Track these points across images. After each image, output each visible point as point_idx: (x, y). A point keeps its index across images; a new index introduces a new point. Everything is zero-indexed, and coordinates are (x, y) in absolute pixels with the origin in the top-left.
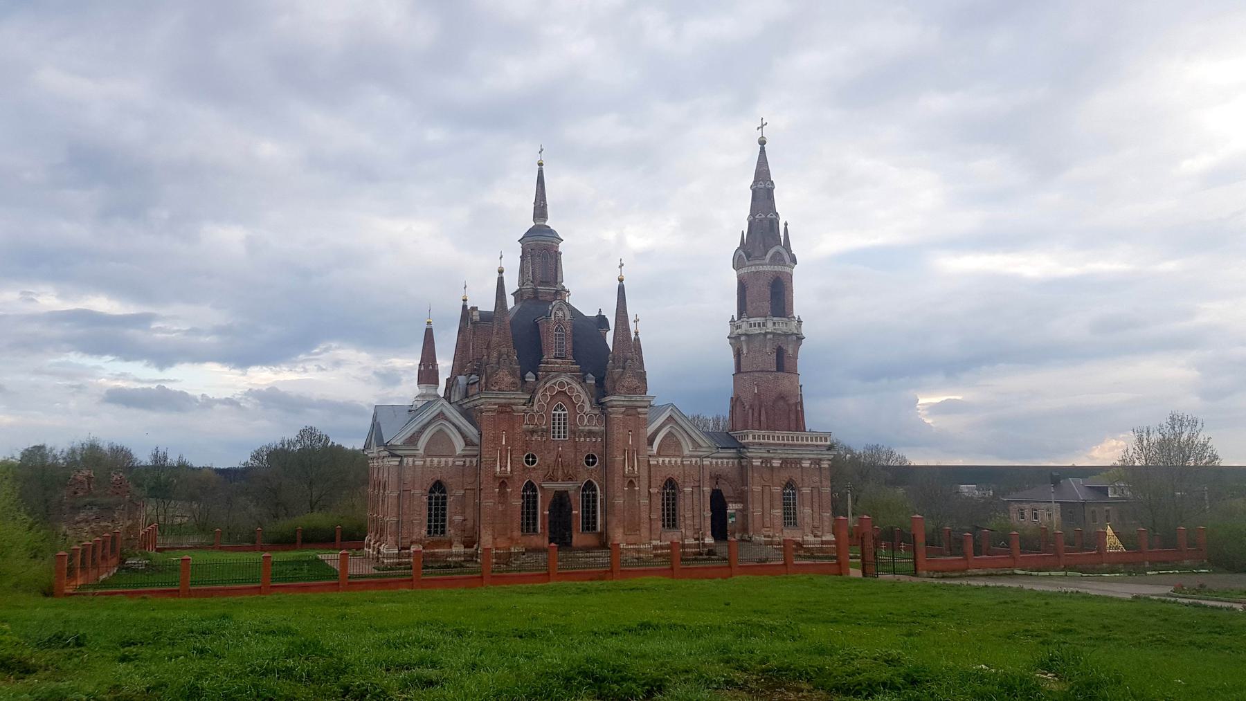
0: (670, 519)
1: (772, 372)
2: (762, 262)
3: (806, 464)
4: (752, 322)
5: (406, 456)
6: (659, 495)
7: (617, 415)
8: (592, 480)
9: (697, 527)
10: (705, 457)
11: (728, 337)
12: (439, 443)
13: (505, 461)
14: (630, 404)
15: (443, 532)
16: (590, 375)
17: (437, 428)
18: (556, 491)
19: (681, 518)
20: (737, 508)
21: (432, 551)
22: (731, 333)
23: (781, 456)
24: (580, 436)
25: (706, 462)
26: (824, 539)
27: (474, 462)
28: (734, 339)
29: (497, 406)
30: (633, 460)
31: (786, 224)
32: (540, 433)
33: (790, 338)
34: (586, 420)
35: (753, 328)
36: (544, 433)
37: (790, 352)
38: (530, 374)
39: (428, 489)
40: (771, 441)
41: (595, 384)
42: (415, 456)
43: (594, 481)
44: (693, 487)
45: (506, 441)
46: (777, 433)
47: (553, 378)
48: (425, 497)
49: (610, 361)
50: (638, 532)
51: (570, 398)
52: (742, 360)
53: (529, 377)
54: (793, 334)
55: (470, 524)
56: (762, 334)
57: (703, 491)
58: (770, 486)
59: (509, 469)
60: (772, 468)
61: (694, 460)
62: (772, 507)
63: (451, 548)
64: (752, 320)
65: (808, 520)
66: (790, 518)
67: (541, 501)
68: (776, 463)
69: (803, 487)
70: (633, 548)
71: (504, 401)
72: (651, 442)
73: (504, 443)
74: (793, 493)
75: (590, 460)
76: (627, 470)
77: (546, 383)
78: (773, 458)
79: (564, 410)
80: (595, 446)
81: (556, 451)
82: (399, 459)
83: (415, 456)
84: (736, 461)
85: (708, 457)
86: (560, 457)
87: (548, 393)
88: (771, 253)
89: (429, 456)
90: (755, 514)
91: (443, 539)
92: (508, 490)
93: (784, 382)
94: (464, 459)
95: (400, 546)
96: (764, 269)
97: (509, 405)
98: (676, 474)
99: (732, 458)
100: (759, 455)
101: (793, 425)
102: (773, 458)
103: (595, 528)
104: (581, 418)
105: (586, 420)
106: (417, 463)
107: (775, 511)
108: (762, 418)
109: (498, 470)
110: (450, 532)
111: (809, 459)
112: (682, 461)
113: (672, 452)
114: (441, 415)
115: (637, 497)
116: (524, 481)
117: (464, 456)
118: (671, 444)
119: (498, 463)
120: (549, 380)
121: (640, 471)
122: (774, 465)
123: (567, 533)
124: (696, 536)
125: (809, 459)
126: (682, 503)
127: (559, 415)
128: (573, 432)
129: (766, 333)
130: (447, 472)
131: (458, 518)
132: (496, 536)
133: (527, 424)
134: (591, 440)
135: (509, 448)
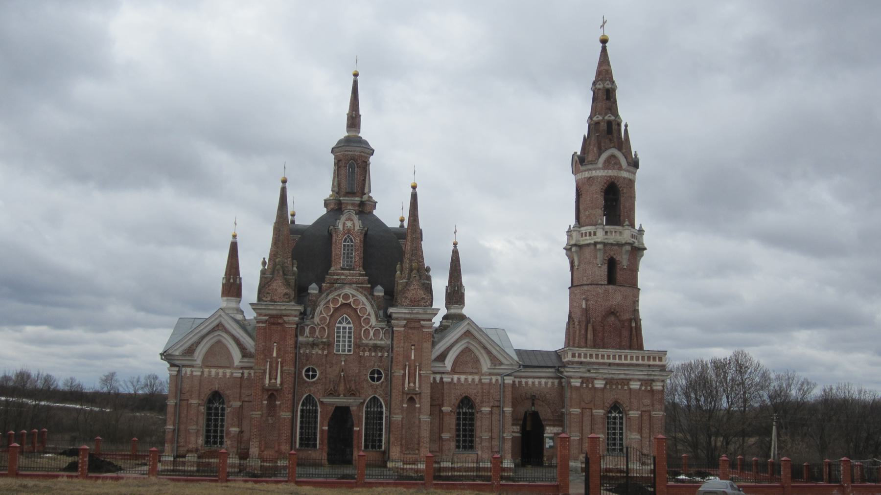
1: (602, 285)
3: (635, 385)
4: (584, 232)
5: (184, 366)
6: (452, 414)
8: (377, 396)
11: (564, 249)
12: (217, 353)
13: (275, 374)
14: (412, 316)
15: (221, 443)
16: (379, 287)
17: (215, 340)
21: (207, 460)
23: (605, 376)
24: (364, 351)
28: (568, 249)
29: (267, 317)
30: (415, 375)
31: (626, 126)
32: (321, 346)
34: (372, 334)
38: (314, 285)
40: (594, 360)
41: (383, 296)
42: (192, 366)
43: (379, 397)
44: (492, 407)
45: (277, 353)
46: (601, 351)
47: (336, 289)
48: (202, 408)
49: (398, 272)
50: (417, 451)
51: (355, 310)
53: (313, 289)
54: (626, 244)
56: (593, 244)
58: (591, 409)
60: (595, 389)
61: (494, 378)
67: (321, 417)
70: (412, 469)
71: (274, 312)
72: (442, 357)
73: (275, 355)
74: (620, 417)
76: (406, 386)
77: (328, 295)
79: (349, 323)
82: (177, 369)
84: (556, 381)
86: (343, 371)
87: (331, 305)
88: (604, 156)
89: (207, 367)
93: (617, 296)
94: (241, 371)
96: (597, 175)
97: (280, 316)
98: (472, 392)
99: (552, 378)
102: (595, 379)
103: (380, 447)
104: (367, 331)
105: (372, 334)
106: (195, 373)
109: (267, 381)
111: (639, 380)
112: (480, 380)
113: (470, 370)
116: (303, 395)
117: (242, 368)
119: (267, 376)
120: (331, 292)
122: (597, 386)
125: (639, 380)
127: (344, 328)
128: (358, 346)
129: (596, 244)
131: (234, 430)
132: (262, 449)
133: (307, 337)
134: (377, 355)
135: (279, 360)
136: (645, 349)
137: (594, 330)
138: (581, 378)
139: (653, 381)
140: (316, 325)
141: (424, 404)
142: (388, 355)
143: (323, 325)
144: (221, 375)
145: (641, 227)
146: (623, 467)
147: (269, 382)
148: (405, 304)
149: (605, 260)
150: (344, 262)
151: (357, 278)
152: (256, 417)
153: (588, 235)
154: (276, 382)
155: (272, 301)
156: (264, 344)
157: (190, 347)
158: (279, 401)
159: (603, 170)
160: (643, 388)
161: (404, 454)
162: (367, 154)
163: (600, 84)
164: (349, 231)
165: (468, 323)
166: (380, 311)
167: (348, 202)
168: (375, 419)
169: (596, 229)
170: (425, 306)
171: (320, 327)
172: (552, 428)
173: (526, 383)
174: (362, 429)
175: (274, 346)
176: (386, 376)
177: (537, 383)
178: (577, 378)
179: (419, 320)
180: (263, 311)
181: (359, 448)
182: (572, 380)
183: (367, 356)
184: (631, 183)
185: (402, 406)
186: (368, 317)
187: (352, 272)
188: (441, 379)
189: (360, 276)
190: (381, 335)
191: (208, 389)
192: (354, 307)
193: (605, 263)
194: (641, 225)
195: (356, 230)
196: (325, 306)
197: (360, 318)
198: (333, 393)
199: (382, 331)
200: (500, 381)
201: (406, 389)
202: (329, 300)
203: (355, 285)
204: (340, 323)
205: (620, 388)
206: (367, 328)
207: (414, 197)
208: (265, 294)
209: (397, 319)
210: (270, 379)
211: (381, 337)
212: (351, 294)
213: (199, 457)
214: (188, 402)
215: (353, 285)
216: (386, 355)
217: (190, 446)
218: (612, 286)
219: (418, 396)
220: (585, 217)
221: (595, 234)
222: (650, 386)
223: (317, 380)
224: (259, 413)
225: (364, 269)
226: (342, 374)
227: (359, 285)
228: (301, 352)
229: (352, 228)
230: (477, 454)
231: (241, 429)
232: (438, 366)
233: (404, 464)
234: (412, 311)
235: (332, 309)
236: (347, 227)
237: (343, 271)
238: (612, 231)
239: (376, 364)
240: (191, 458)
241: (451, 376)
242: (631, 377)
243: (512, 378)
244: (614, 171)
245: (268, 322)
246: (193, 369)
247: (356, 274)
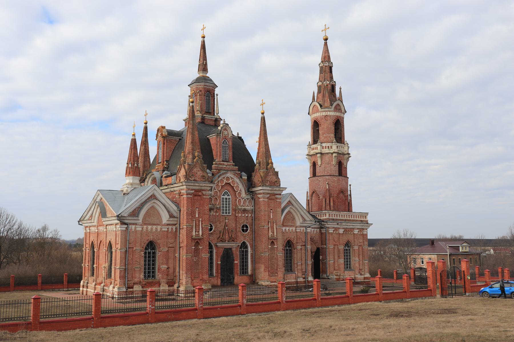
0: (289, 267)
1: (336, 176)
2: (329, 109)
3: (356, 232)
4: (324, 146)
7: (262, 198)
8: (245, 241)
9: (304, 270)
14: (272, 192)
16: (243, 173)
17: (151, 206)
18: (225, 249)
19: (295, 265)
22: (309, 152)
25: (309, 230)
26: (366, 276)
27: (174, 229)
31: (340, 89)
35: (325, 149)
36: (218, 210)
39: (145, 247)
42: (136, 224)
46: (342, 213)
47: (223, 174)
51: (233, 187)
52: (317, 169)
55: (171, 270)
59: (201, 233)
61: (302, 229)
62: (339, 257)
63: (159, 287)
64: (324, 145)
65: (357, 265)
66: (348, 266)
67: (216, 255)
68: (341, 231)
69: (354, 245)
71: (197, 188)
73: (197, 216)
75: (245, 228)
77: (219, 177)
79: (228, 195)
80: (247, 220)
81: (224, 223)
82: (126, 226)
83: (136, 224)
84: (318, 230)
85: (309, 227)
86: (227, 226)
90: (330, 262)
91: (155, 281)
92: (200, 247)
95: (126, 286)
98: (292, 237)
99: (316, 228)
100: (333, 226)
101: (347, 209)
103: (247, 272)
106: (137, 229)
107: (340, 260)
109: (194, 234)
110: (159, 276)
111: (358, 229)
112: (296, 230)
113: (291, 224)
114: (153, 197)
115: (276, 251)
118: (289, 219)
119: (194, 230)
121: (278, 236)
122: (340, 232)
123: (231, 276)
124: (304, 276)
125: (358, 229)
126: (295, 256)
128: (235, 210)
129: (332, 154)
130: (157, 236)
131: (164, 267)
132: (193, 279)
134: (245, 215)
135: (201, 219)
136: (353, 212)
137: (334, 201)
138: (333, 228)
140: (212, 197)
141: (280, 246)
146: (353, 277)
148: (267, 184)
149: (337, 162)
152: (189, 258)
153: (324, 147)
154: (199, 234)
155: (194, 180)
156: (191, 209)
158: (201, 246)
161: (270, 276)
163: (326, 63)
167: (212, 119)
170: (277, 186)
171: (214, 198)
176: (250, 228)
178: (331, 228)
180: (191, 187)
181: (237, 274)
183: (240, 216)
185: (268, 247)
187: (228, 163)
190: (247, 203)
191: (146, 240)
192: (233, 185)
195: (229, 136)
198: (223, 241)
201: (270, 236)
202: (219, 181)
206: (240, 198)
207: (263, 120)
208: (191, 176)
213: (142, 287)
214: (133, 250)
217: (136, 280)
218: (341, 177)
219: (276, 240)
220: (323, 138)
221: (331, 148)
223: (213, 232)
224: (190, 254)
227: (234, 172)
229: (227, 135)
230: (296, 274)
237: (224, 163)
239: (245, 221)
240: (137, 288)
243: (311, 228)
246: (137, 227)
247: (231, 164)
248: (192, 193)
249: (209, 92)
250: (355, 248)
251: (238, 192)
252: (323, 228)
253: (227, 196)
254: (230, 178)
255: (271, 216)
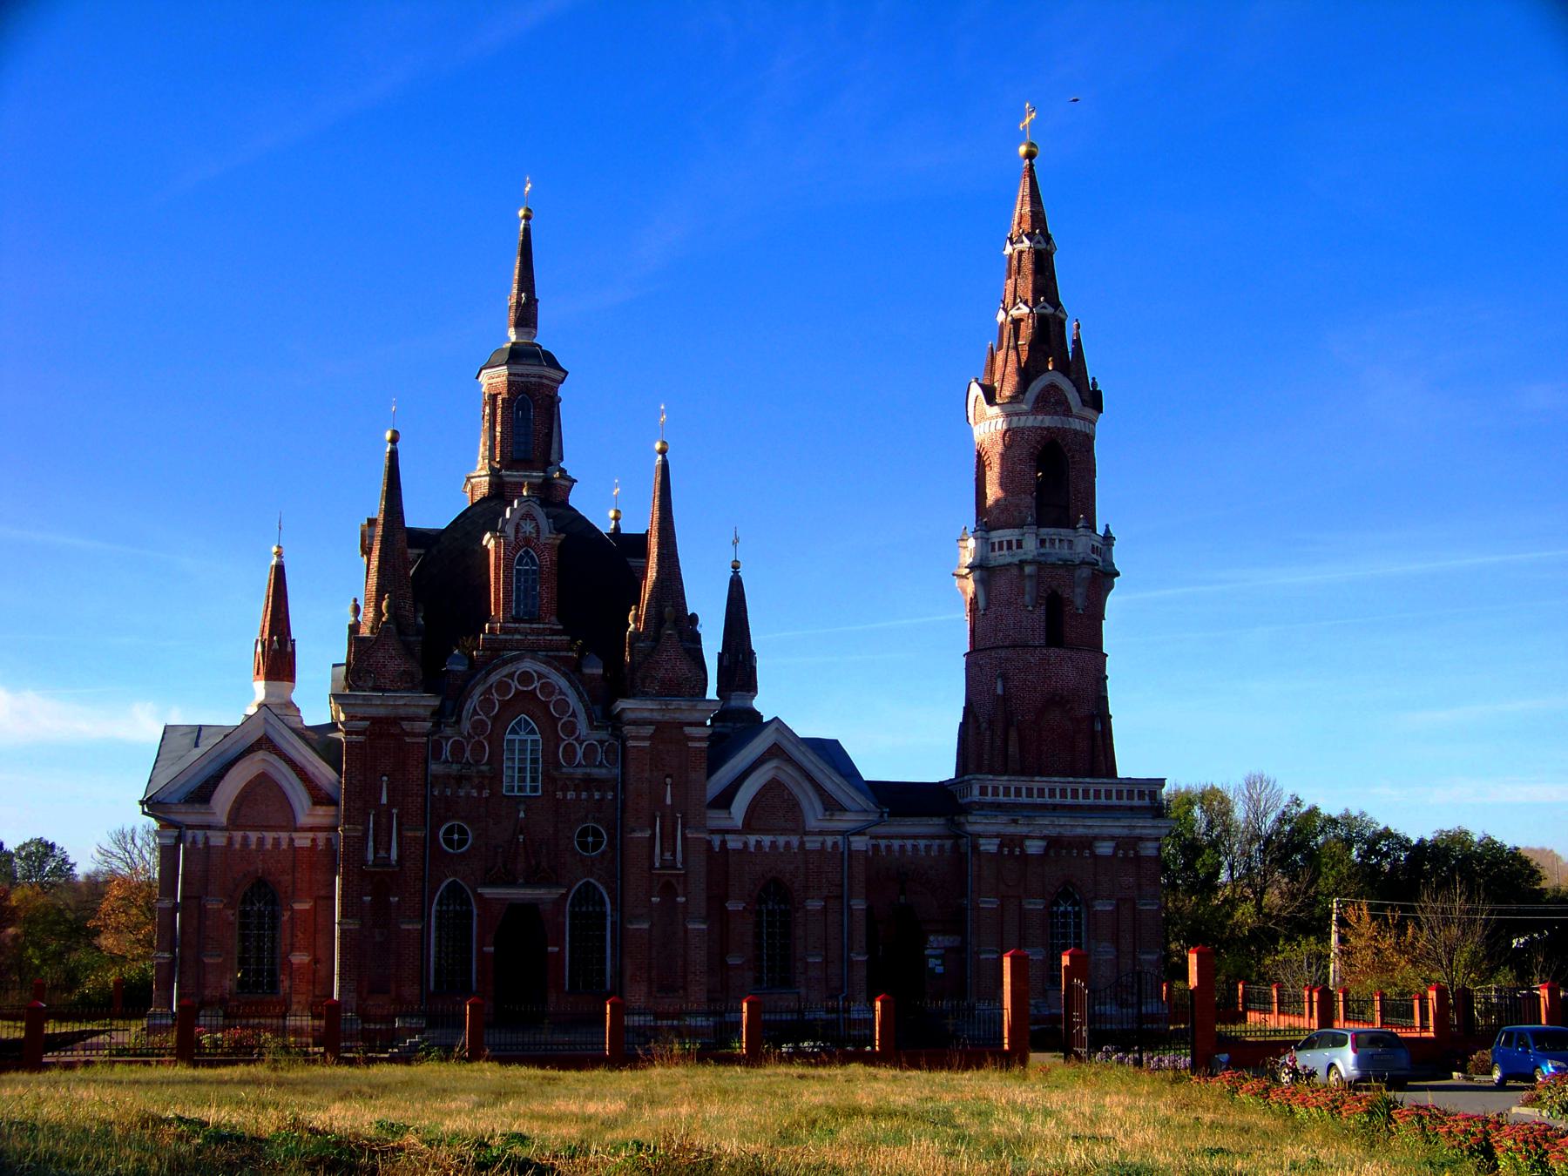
3: (1105, 849)
4: (996, 540)
7: (639, 740)
8: (592, 880)
10: (853, 834)
20: (947, 944)
23: (1046, 832)
24: (565, 789)
29: (368, 723)
32: (476, 781)
33: (1078, 572)
36: (486, 782)
37: (1079, 602)
42: (209, 827)
43: (597, 884)
44: (826, 899)
46: (1038, 782)
47: (505, 663)
51: (547, 705)
54: (1083, 563)
56: (1016, 565)
57: (849, 907)
61: (829, 840)
69: (1095, 898)
71: (382, 712)
72: (724, 800)
73: (384, 800)
77: (488, 674)
78: (1028, 837)
79: (532, 732)
82: (175, 832)
83: (209, 827)
84: (948, 843)
86: (521, 833)
89: (239, 828)
93: (1065, 668)
97: (395, 721)
99: (939, 837)
102: (1028, 837)
108: (1011, 749)
109: (371, 856)
112: (802, 844)
116: (441, 881)
119: (371, 844)
120: (495, 668)
122: (1030, 851)
125: (1112, 838)
129: (1022, 563)
139: (1140, 839)
142: (615, 797)
143: (479, 736)
144: (269, 845)
145: (1107, 530)
147: (374, 856)
150: (518, 605)
151: (547, 638)
154: (389, 857)
157: (201, 787)
159: (1033, 415)
160: (1120, 854)
162: (554, 380)
164: (528, 541)
165: (777, 729)
166: (595, 707)
168: (588, 925)
169: (1023, 535)
171: (473, 740)
172: (940, 938)
173: (888, 847)
174: (564, 948)
175: (382, 781)
177: (909, 847)
179: (682, 724)
182: (982, 841)
183: (571, 799)
184: (1087, 441)
186: (571, 719)
187: (535, 626)
188: (724, 843)
189: (553, 635)
192: (543, 699)
193: (1041, 605)
194: (1107, 526)
195: (542, 540)
196: (482, 697)
197: (555, 720)
199: (602, 747)
200: (840, 843)
202: (491, 685)
203: (544, 653)
204: (513, 731)
205: (1075, 855)
206: (571, 741)
209: (635, 723)
210: (376, 851)
211: (599, 759)
212: (535, 671)
215: (540, 653)
216: (610, 797)
221: (1019, 545)
222: (1134, 849)
223: (467, 850)
225: (561, 621)
226: (521, 837)
227: (551, 654)
228: (436, 793)
229: (534, 535)
230: (798, 993)
231: (315, 955)
232: (716, 819)
233: (656, 1018)
234: (666, 705)
235: (497, 702)
236: (525, 532)
237: (517, 625)
238: (1054, 540)
239: (590, 816)
241: (743, 838)
242: (1097, 831)
244: (1055, 417)
245: (368, 733)
248: (366, 729)
249: (526, 393)
250: (1099, 908)
251: (563, 721)
252: (961, 837)
253: (528, 733)
254: (535, 674)
255: (665, 799)
